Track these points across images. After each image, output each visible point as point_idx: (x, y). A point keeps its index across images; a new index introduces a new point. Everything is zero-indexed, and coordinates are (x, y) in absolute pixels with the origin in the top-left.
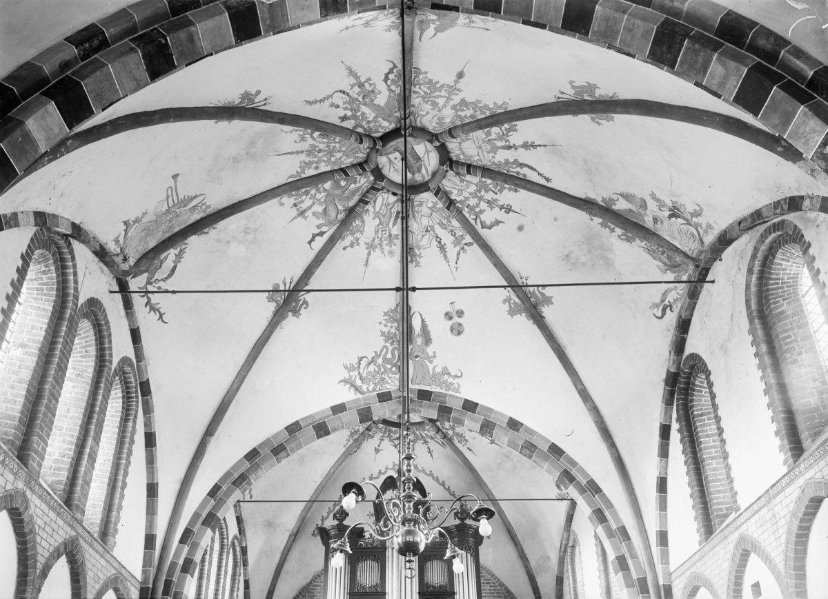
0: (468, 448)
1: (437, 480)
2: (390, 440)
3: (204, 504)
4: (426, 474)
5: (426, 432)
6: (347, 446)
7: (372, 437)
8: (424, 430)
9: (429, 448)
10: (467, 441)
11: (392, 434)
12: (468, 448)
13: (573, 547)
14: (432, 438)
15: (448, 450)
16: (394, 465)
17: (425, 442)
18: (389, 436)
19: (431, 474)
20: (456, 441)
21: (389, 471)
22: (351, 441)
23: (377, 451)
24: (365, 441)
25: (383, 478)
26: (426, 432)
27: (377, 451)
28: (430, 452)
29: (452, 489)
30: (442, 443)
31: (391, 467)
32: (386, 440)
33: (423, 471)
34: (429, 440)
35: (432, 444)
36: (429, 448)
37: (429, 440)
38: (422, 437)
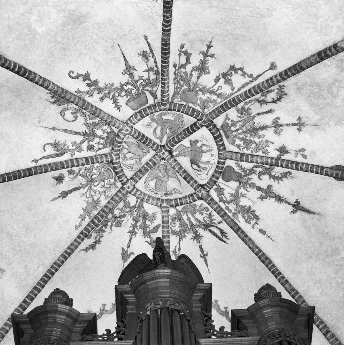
0: (261, 230)
7: (119, 224)
8: (193, 213)
10: (257, 218)
11: (148, 223)
12: (261, 230)
14: (206, 226)
17: (197, 237)
18: (144, 227)
22: (87, 220)
24: (108, 229)
26: (197, 215)
30: (222, 232)
32: (139, 232)
34: (201, 231)
37: (201, 231)
38: (192, 225)
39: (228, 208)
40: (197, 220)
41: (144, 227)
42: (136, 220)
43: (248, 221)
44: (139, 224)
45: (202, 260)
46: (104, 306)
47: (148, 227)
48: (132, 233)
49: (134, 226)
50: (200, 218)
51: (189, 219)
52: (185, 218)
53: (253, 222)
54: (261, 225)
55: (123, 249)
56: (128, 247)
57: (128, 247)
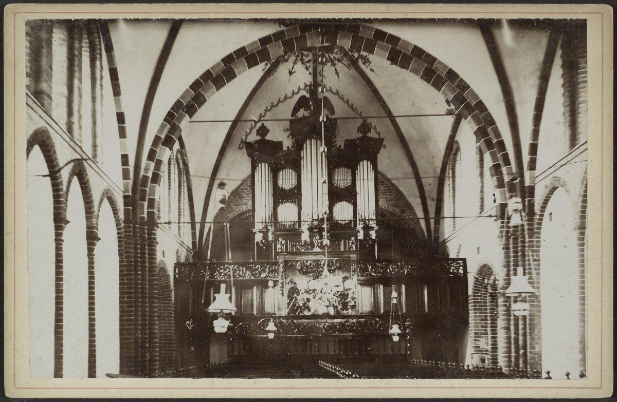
1: (342, 98)
2: (303, 63)
3: (162, 127)
4: (333, 93)
5: (334, 55)
6: (266, 70)
7: (287, 61)
9: (336, 70)
10: (370, 62)
11: (304, 57)
13: (456, 154)
14: (339, 60)
15: (353, 71)
16: (306, 86)
17: (333, 64)
18: (302, 59)
19: (337, 93)
20: (360, 63)
21: (301, 91)
23: (291, 73)
25: (296, 98)
26: (334, 55)
27: (291, 73)
28: (337, 73)
29: (355, 106)
31: (302, 87)
32: (299, 63)
33: (331, 90)
34: (336, 62)
35: (339, 66)
36: (336, 70)
37: (336, 62)
38: (330, 59)
39: (353, 55)
40: (334, 57)
41: (302, 59)
42: (298, 56)
43: (364, 63)
44: (299, 59)
45: (336, 76)
46: (279, 99)
47: (304, 60)
48: (295, 63)
49: (296, 60)
50: (336, 57)
51: (329, 56)
52: (327, 56)
53: (367, 65)
54: (372, 66)
55: (289, 71)
56: (292, 69)
57: (292, 69)
